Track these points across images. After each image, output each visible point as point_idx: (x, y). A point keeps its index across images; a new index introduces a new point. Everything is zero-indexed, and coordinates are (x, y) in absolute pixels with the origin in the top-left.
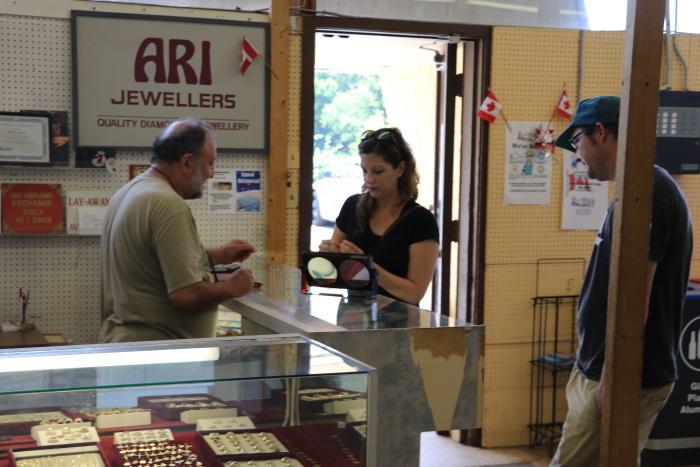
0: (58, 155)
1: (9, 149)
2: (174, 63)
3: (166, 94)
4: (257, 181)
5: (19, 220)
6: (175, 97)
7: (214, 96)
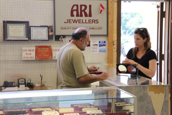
0: (50, 37)
1: (37, 36)
2: (81, 11)
3: (79, 20)
4: (105, 44)
5: (40, 56)
6: (82, 21)
7: (92, 20)
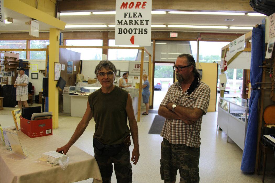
2: (139, 66)
